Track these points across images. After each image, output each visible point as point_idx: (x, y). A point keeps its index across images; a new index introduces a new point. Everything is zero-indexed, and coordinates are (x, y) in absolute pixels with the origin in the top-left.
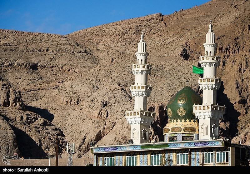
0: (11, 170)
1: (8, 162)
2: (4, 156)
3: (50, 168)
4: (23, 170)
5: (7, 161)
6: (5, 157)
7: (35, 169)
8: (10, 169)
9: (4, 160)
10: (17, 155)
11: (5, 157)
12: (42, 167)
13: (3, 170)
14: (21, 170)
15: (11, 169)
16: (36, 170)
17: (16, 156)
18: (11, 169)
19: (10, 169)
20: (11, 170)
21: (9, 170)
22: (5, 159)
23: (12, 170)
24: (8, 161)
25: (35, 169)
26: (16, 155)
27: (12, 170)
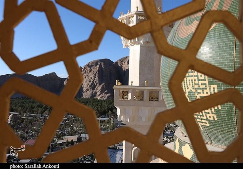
0: (19, 166)
1: (15, 154)
2: (12, 147)
3: (61, 165)
4: (31, 167)
5: (14, 153)
6: (13, 149)
7: (44, 165)
8: (18, 165)
9: (11, 152)
10: (25, 147)
11: (13, 149)
12: (51, 164)
13: (11, 166)
14: (29, 167)
15: (18, 166)
16: (45, 166)
17: (24, 148)
18: (18, 166)
19: (18, 165)
20: (19, 166)
21: (17, 167)
22: (13, 151)
23: (21, 167)
24: (15, 153)
25: (44, 165)
26: (23, 147)
27: (21, 167)
